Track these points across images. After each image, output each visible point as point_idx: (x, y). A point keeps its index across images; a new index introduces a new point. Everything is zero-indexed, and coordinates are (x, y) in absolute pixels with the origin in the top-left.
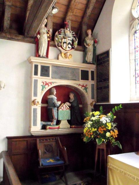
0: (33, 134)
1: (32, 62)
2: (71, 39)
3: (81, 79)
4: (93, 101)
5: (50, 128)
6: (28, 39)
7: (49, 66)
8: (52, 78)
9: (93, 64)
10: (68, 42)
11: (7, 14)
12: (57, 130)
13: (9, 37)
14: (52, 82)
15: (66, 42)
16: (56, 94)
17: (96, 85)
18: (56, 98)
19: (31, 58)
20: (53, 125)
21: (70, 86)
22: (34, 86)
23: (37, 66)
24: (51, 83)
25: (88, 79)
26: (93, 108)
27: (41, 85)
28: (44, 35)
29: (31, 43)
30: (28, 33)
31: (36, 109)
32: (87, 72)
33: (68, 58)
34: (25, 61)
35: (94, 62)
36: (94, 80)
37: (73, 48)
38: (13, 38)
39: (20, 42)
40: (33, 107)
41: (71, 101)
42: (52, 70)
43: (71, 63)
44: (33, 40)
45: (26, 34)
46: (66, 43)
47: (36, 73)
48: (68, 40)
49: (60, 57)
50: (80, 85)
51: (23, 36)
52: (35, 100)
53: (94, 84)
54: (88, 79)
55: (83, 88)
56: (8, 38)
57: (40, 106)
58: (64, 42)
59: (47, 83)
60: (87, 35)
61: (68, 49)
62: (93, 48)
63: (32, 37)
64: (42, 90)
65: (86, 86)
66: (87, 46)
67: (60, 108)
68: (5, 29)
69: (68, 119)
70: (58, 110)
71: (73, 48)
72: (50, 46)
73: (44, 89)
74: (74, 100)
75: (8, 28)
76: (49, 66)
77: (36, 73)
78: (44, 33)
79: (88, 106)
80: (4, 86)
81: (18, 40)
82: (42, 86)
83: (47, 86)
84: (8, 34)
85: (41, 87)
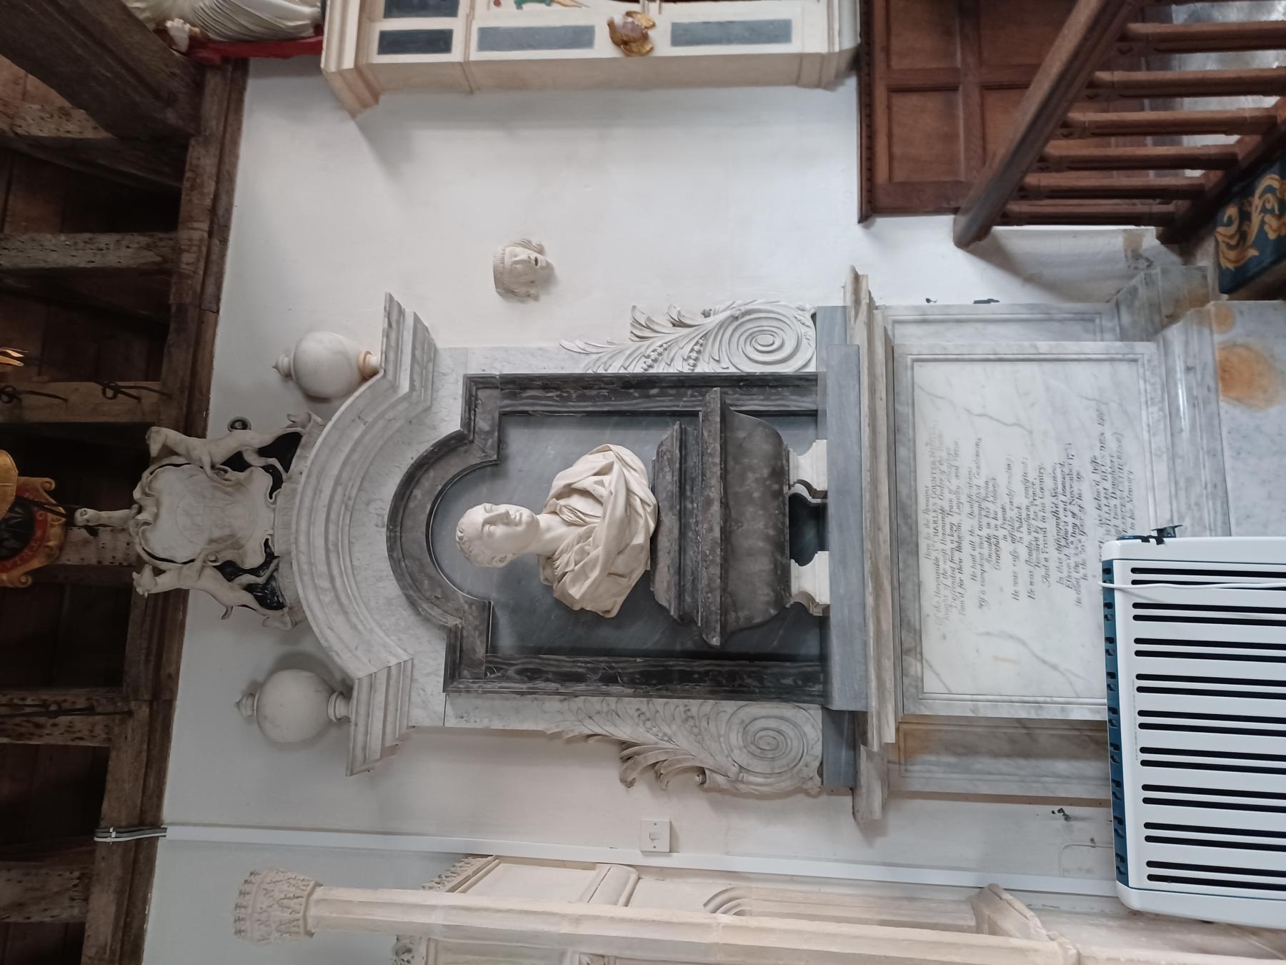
1: (357, 68)
6: (211, 108)
11: (54, 255)
13: (205, 226)
19: (333, 68)
23: (383, 35)
29: (240, 101)
30: (170, 101)
34: (363, 129)
38: (208, 202)
40: (662, 45)
44: (213, 82)
45: (171, 117)
47: (440, 41)
51: (192, 142)
52: (611, 25)
56: (210, 234)
63: (198, 87)
68: (151, 257)
75: (143, 240)
77: (440, 41)
80: (526, 244)
81: (225, 178)
84: (183, 235)
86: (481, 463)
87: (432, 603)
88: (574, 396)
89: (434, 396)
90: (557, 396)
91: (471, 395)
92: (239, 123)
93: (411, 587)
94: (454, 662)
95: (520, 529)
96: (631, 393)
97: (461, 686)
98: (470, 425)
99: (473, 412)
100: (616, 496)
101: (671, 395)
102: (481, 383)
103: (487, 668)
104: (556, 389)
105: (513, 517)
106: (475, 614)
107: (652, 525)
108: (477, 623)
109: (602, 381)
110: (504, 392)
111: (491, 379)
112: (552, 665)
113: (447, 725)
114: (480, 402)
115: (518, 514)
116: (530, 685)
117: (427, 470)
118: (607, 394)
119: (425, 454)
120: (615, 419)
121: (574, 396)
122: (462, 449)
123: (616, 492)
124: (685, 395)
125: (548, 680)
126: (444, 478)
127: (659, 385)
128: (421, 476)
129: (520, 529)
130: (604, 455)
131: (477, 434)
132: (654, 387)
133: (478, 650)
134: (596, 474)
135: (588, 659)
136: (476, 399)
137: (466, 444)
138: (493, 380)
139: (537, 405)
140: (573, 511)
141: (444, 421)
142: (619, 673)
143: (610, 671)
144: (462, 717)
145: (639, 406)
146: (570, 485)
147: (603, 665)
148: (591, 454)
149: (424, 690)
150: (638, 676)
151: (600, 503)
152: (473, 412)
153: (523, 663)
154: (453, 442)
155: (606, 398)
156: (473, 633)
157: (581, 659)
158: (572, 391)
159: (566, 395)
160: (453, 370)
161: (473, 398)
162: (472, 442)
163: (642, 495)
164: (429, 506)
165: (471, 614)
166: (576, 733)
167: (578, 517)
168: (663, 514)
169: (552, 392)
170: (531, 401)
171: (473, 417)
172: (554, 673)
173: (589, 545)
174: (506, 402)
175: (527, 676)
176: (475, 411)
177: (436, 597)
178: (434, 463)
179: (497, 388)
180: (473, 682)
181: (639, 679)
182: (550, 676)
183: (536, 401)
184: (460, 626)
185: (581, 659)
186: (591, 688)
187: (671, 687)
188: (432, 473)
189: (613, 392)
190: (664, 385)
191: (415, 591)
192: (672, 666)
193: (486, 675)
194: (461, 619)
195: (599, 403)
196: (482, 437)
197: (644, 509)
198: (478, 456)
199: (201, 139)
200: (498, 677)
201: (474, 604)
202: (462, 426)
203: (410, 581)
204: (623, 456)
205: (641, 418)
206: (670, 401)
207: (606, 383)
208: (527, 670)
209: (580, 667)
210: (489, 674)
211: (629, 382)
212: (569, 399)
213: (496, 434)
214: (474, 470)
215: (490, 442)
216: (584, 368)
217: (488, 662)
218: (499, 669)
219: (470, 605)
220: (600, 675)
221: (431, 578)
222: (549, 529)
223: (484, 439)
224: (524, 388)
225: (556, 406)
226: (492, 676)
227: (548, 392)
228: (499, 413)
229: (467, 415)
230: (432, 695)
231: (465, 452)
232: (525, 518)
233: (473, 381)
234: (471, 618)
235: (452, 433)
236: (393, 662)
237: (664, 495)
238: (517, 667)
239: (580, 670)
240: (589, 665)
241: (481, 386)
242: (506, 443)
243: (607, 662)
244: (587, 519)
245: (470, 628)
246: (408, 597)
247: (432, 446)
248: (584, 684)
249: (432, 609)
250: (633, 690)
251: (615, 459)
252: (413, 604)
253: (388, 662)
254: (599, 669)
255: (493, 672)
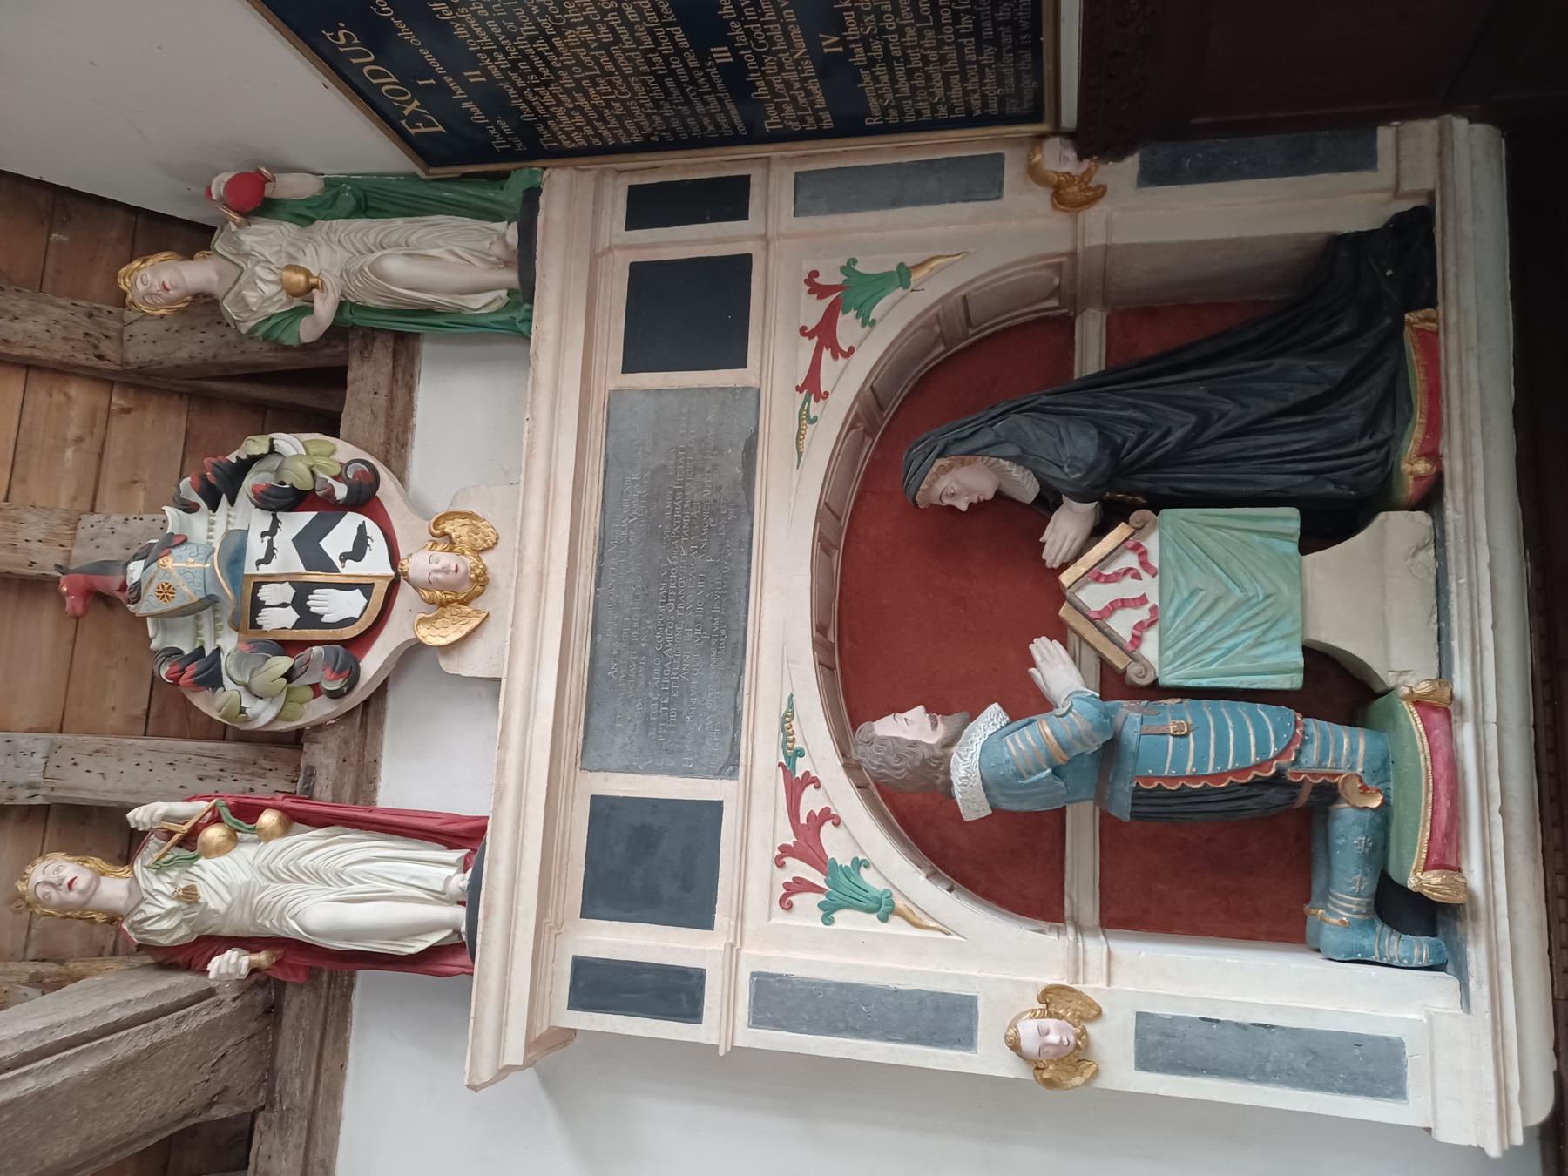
0: (1541, 1108)
2: (262, 521)
3: (742, 364)
4: (1034, 173)
5: (1445, 856)
6: (292, 1055)
7: (595, 800)
8: (729, 766)
9: (531, 198)
10: (288, 560)
12: (1466, 735)
14: (787, 769)
15: (288, 592)
16: (936, 708)
17: (803, 148)
18: (993, 717)
20: (1383, 768)
21: (826, 511)
22: (833, 1030)
23: (581, 966)
24: (795, 787)
25: (739, 267)
26: (1132, 163)
27: (827, 919)
28: (205, 895)
29: (345, 1012)
31: (1139, 1035)
32: (643, 277)
33: (487, 558)
35: (512, 194)
36: (745, 181)
37: (364, 499)
39: (333, 1143)
41: (1026, 487)
42: (629, 769)
43: (534, 524)
44: (297, 1005)
46: (303, 591)
48: (267, 559)
49: (474, 663)
50: (811, 386)
51: (260, 1123)
53: (801, 179)
54: (739, 267)
55: (847, 328)
57: (1096, 947)
58: (291, 616)
59: (790, 839)
60: (204, 305)
61: (376, 563)
62: (341, 224)
64: (883, 908)
65: (819, 291)
66: (325, 308)
67: (1119, 660)
69: (1292, 548)
70: (1156, 691)
71: (364, 499)
72: (366, 776)
73: (867, 876)
74: (1017, 460)
76: (595, 800)
78: (189, 896)
79: (1097, 239)
82: (828, 911)
83: (833, 842)
85: (845, 920)
92: (343, 1053)
199: (274, 1117)
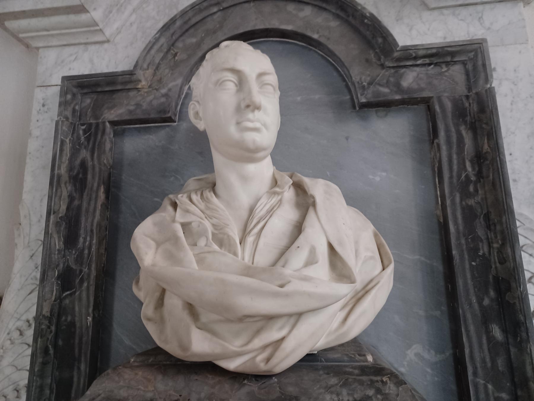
86: (353, 84)
87: (169, 50)
88: (471, 202)
89: (445, 11)
90: (467, 176)
91: (453, 54)
93: (186, 23)
94: (97, 85)
95: (233, 130)
96: (487, 293)
97: (69, 97)
98: (407, 59)
99: (427, 61)
100: (276, 295)
101: (493, 361)
102: (475, 67)
103: (90, 125)
104: (480, 175)
105: (251, 116)
106: (155, 103)
107: (232, 365)
108: (145, 106)
109: (503, 245)
110: (464, 99)
111: (482, 75)
112: (89, 204)
113: (37, 90)
114: (445, 69)
115: (258, 125)
116: (65, 177)
117: (338, 16)
118: (481, 253)
119: (359, 8)
120: (439, 266)
121: (471, 202)
122: (372, 56)
123: (287, 295)
124: (499, 388)
125: (71, 198)
126: (329, 39)
127: (511, 340)
128: (330, 11)
129: (233, 130)
130: (372, 258)
131: (396, 72)
132: (504, 331)
133: (112, 112)
134: (331, 247)
135: (94, 249)
136: (447, 64)
137: (379, 59)
138: (481, 82)
139: (450, 148)
140: (271, 212)
141: (411, 29)
142: (75, 292)
143: (77, 281)
144: (44, 105)
145: (466, 307)
146: (314, 205)
147: (86, 270)
148: (376, 235)
149: (76, 59)
150: (69, 318)
151: (274, 264)
152: (427, 61)
153: (93, 167)
154: (380, 40)
155: (474, 252)
156: (133, 103)
157: (94, 241)
158: (479, 198)
159: (471, 189)
160: (489, 29)
161: (449, 59)
162: (382, 66)
163: (288, 345)
164: (289, 27)
165: (154, 98)
166: (16, 241)
167: (258, 222)
168: (253, 387)
169: (473, 169)
170: (454, 139)
171: (419, 62)
172: (79, 207)
173: (206, 245)
174: (449, 105)
175: (78, 174)
176: (430, 64)
177: (176, 54)
178: (350, 24)
179: (469, 89)
180: (74, 111)
181: (66, 320)
182: (76, 203)
183: (455, 147)
184: (139, 86)
185: (94, 241)
186: (55, 257)
187: (49, 369)
188: (334, 23)
189: (486, 263)
190: (513, 350)
191: (181, 27)
192: (79, 368)
193: (83, 125)
194: (150, 87)
195: (463, 241)
196: (392, 79)
197: (265, 347)
198: (363, 78)
200: (79, 138)
201: (167, 99)
202: (406, 49)
203: (194, 21)
204: (373, 292)
205: (444, 308)
206: (484, 361)
207: (500, 251)
208: (85, 173)
209: (85, 239)
210: (84, 127)
211: (509, 289)
212: (465, 194)
213: (398, 97)
214: (344, 80)
215: (386, 90)
216: (521, 214)
217: (97, 125)
218: (88, 139)
219: (166, 95)
220: (74, 267)
221: (198, 45)
222: (245, 179)
223: (388, 82)
224: (473, 128)
225: (451, 177)
226: (81, 132)
227: (471, 161)
228: (430, 98)
229: (421, 53)
230: (70, 69)
231: (367, 61)
232: (251, 137)
233: (476, 56)
234: (151, 97)
235: (391, 35)
236: (97, 15)
237: (291, 390)
238: (89, 158)
239: (81, 240)
240: (86, 252)
241: (470, 66)
242: (386, 115)
243: (89, 275)
244: (250, 239)
245: (139, 98)
246: (173, 21)
247: (372, 15)
248: (62, 246)
249: (159, 51)
250: (49, 314)
251: (360, 279)
252: (166, 27)
253: (95, 9)
254: (81, 264)
255: (85, 132)
